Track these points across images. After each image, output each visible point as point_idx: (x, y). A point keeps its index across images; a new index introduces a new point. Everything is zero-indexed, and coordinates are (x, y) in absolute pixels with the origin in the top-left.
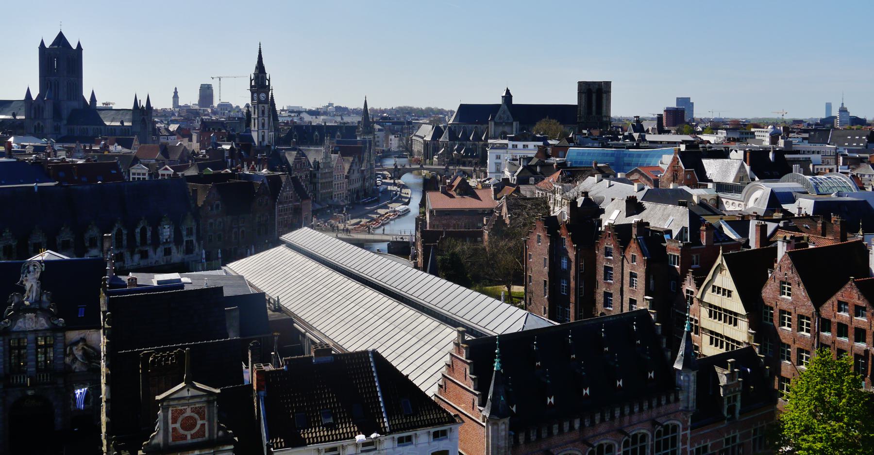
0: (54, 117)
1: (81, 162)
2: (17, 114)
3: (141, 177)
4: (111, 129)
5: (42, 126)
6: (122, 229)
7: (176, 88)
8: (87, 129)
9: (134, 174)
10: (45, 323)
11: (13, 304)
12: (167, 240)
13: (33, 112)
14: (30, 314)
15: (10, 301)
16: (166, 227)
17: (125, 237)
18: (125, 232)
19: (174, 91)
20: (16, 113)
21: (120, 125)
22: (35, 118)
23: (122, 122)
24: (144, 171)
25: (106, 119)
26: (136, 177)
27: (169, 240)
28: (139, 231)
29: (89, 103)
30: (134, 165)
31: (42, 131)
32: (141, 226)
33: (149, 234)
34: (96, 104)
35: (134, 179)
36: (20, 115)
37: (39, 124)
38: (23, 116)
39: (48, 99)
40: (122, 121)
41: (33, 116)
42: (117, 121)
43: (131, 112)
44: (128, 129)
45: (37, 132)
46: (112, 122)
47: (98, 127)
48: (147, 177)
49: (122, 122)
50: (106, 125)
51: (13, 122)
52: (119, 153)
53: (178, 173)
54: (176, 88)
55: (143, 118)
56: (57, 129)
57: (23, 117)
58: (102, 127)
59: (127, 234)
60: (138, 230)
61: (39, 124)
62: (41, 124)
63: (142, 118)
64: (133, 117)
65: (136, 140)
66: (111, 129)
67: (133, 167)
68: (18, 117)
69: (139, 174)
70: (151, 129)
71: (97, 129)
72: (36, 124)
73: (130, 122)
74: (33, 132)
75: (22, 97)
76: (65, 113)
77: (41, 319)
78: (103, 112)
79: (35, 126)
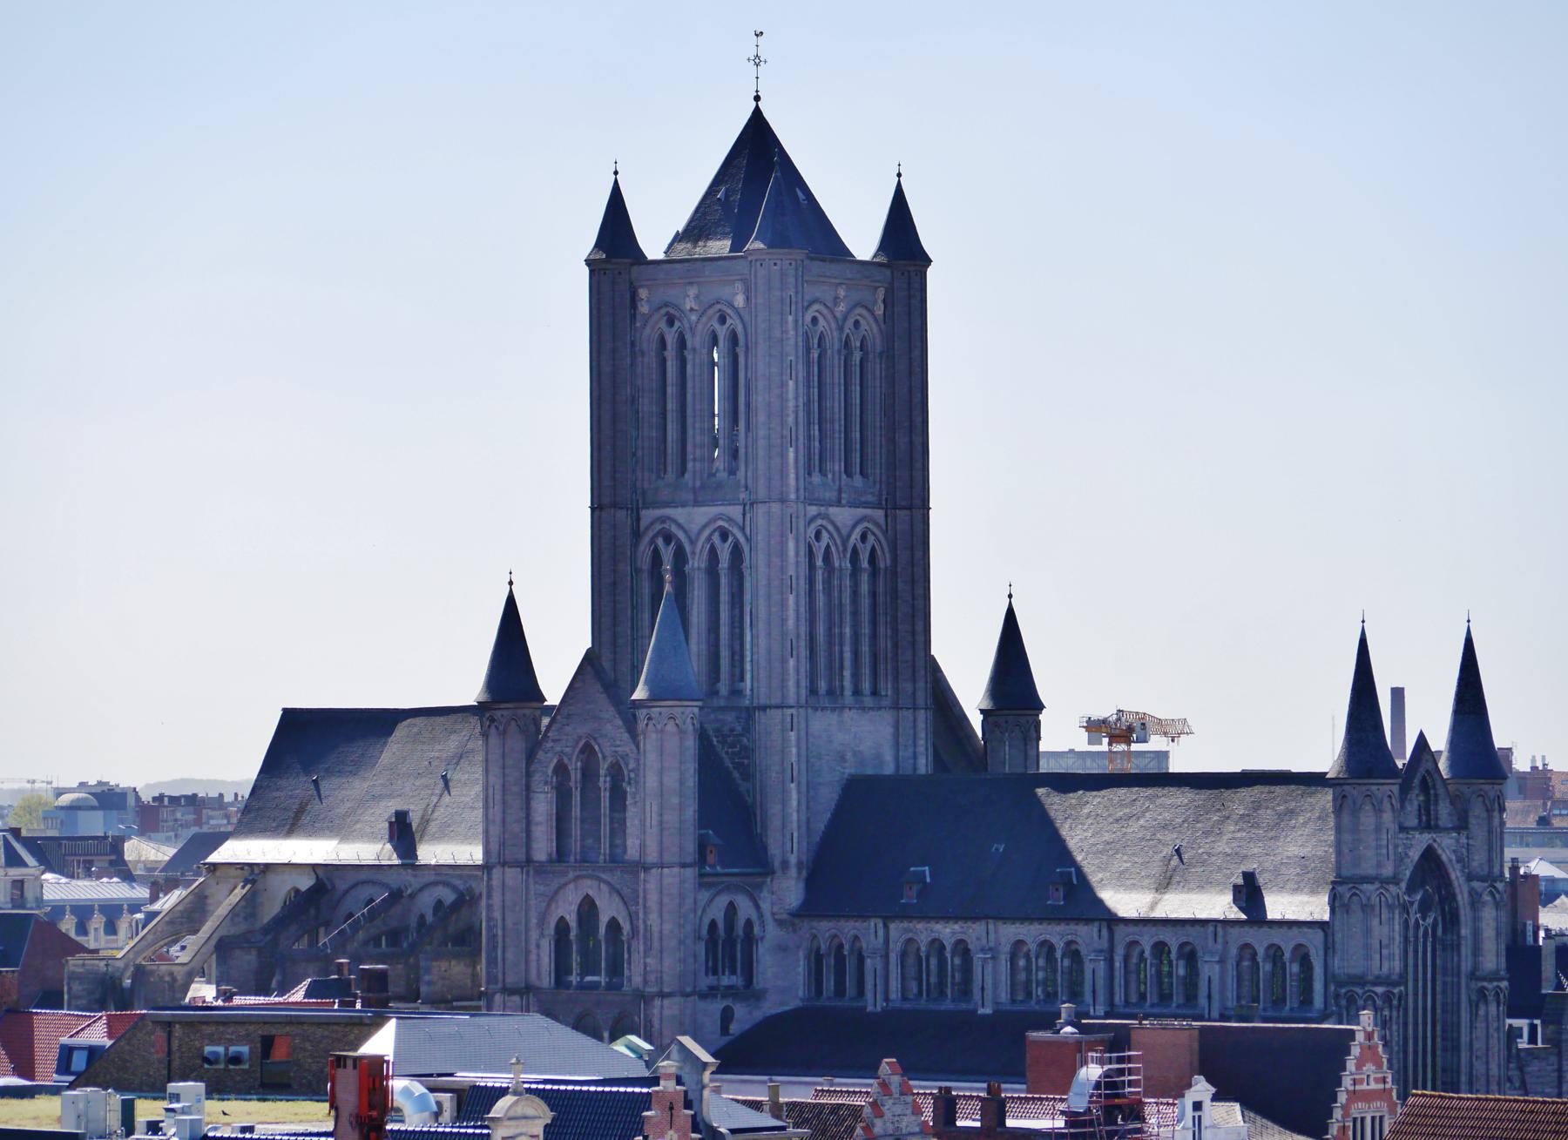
2: (425, 821)
4: (1160, 948)
5: (614, 925)
8: (962, 949)
13: (543, 805)
20: (415, 822)
21: (1236, 914)
22: (561, 854)
23: (1249, 894)
25: (1121, 863)
29: (976, 721)
31: (616, 968)
34: (1032, 732)
36: (444, 835)
37: (588, 909)
38: (466, 839)
39: (656, 696)
40: (1249, 877)
41: (543, 848)
42: (1204, 885)
43: (1326, 798)
45: (574, 978)
46: (1164, 884)
47: (1056, 934)
49: (1249, 894)
50: (1112, 920)
51: (396, 896)
55: (1429, 855)
57: (471, 853)
58: (1087, 936)
61: (588, 909)
62: (609, 910)
63: (1415, 854)
64: (1338, 844)
65: (1369, 1052)
66: (1160, 948)
68: (430, 853)
70: (1492, 958)
71: (1047, 947)
72: (567, 907)
73: (1314, 891)
74: (546, 980)
78: (1095, 801)
79: (562, 927)
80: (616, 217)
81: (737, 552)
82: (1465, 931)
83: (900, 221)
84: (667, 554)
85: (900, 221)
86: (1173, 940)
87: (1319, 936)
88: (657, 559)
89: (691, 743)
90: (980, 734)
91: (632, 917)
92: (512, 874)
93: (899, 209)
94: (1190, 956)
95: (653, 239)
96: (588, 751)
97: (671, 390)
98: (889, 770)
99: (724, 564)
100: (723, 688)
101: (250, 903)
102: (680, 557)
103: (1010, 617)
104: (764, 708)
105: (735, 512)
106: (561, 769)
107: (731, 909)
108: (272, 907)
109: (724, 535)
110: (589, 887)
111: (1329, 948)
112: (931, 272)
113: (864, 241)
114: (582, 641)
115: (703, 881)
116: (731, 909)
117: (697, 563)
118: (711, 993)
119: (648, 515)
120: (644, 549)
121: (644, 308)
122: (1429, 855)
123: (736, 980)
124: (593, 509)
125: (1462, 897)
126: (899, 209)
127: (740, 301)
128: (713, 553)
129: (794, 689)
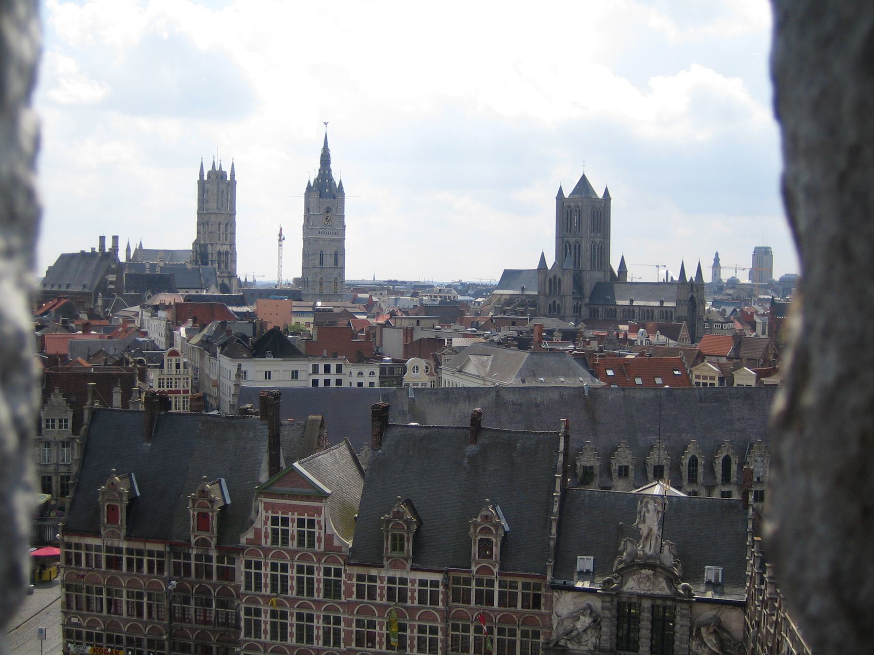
0: (573, 293)
1: (633, 357)
3: (708, 381)
4: (648, 311)
5: (558, 305)
6: (697, 456)
7: (717, 254)
9: (698, 377)
10: (666, 587)
11: (625, 554)
12: (758, 479)
13: (547, 285)
14: (647, 570)
15: (621, 548)
16: (759, 459)
17: (700, 470)
18: (701, 461)
19: (714, 256)
24: (712, 374)
26: (701, 381)
27: (761, 480)
28: (721, 462)
29: (617, 273)
30: (697, 364)
31: (559, 312)
32: (724, 454)
33: (734, 467)
35: (698, 384)
37: (554, 302)
38: (535, 291)
43: (675, 287)
44: (671, 312)
48: (716, 383)
49: (662, 302)
52: (664, 345)
53: (762, 379)
54: (717, 254)
55: (692, 296)
56: (577, 309)
59: (705, 466)
60: (719, 462)
61: (554, 302)
62: (558, 302)
66: (648, 311)
67: (697, 367)
69: (705, 378)
72: (551, 302)
74: (547, 314)
75: (534, 265)
76: (588, 289)
77: (661, 579)
79: (550, 305)
80: (561, 192)
81: (579, 246)
82: (697, 308)
83: (606, 193)
84: (568, 245)
85: (606, 193)
86: (649, 309)
87: (673, 310)
88: (566, 246)
89: (572, 276)
90: (617, 275)
91: (562, 304)
92: (543, 296)
93: (606, 190)
94: (652, 312)
95: (567, 194)
96: (555, 277)
97: (569, 219)
98: (603, 281)
99: (577, 247)
100: (577, 267)
101: (499, 301)
102: (570, 246)
103: (623, 257)
104: (583, 271)
105: (579, 239)
106: (550, 280)
107: (578, 303)
108: (502, 301)
109: (577, 242)
110: (554, 299)
111: (675, 311)
112: (611, 200)
113: (600, 194)
114: (554, 260)
115: (574, 298)
116: (578, 303)
117: (573, 247)
118: (574, 316)
119: (565, 239)
120: (564, 244)
121: (565, 205)
122: (692, 296)
123: (578, 314)
124: (556, 238)
125: (697, 303)
126: (606, 190)
127: (581, 204)
128: (575, 246)
129: (588, 268)
